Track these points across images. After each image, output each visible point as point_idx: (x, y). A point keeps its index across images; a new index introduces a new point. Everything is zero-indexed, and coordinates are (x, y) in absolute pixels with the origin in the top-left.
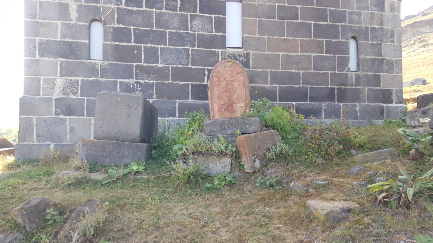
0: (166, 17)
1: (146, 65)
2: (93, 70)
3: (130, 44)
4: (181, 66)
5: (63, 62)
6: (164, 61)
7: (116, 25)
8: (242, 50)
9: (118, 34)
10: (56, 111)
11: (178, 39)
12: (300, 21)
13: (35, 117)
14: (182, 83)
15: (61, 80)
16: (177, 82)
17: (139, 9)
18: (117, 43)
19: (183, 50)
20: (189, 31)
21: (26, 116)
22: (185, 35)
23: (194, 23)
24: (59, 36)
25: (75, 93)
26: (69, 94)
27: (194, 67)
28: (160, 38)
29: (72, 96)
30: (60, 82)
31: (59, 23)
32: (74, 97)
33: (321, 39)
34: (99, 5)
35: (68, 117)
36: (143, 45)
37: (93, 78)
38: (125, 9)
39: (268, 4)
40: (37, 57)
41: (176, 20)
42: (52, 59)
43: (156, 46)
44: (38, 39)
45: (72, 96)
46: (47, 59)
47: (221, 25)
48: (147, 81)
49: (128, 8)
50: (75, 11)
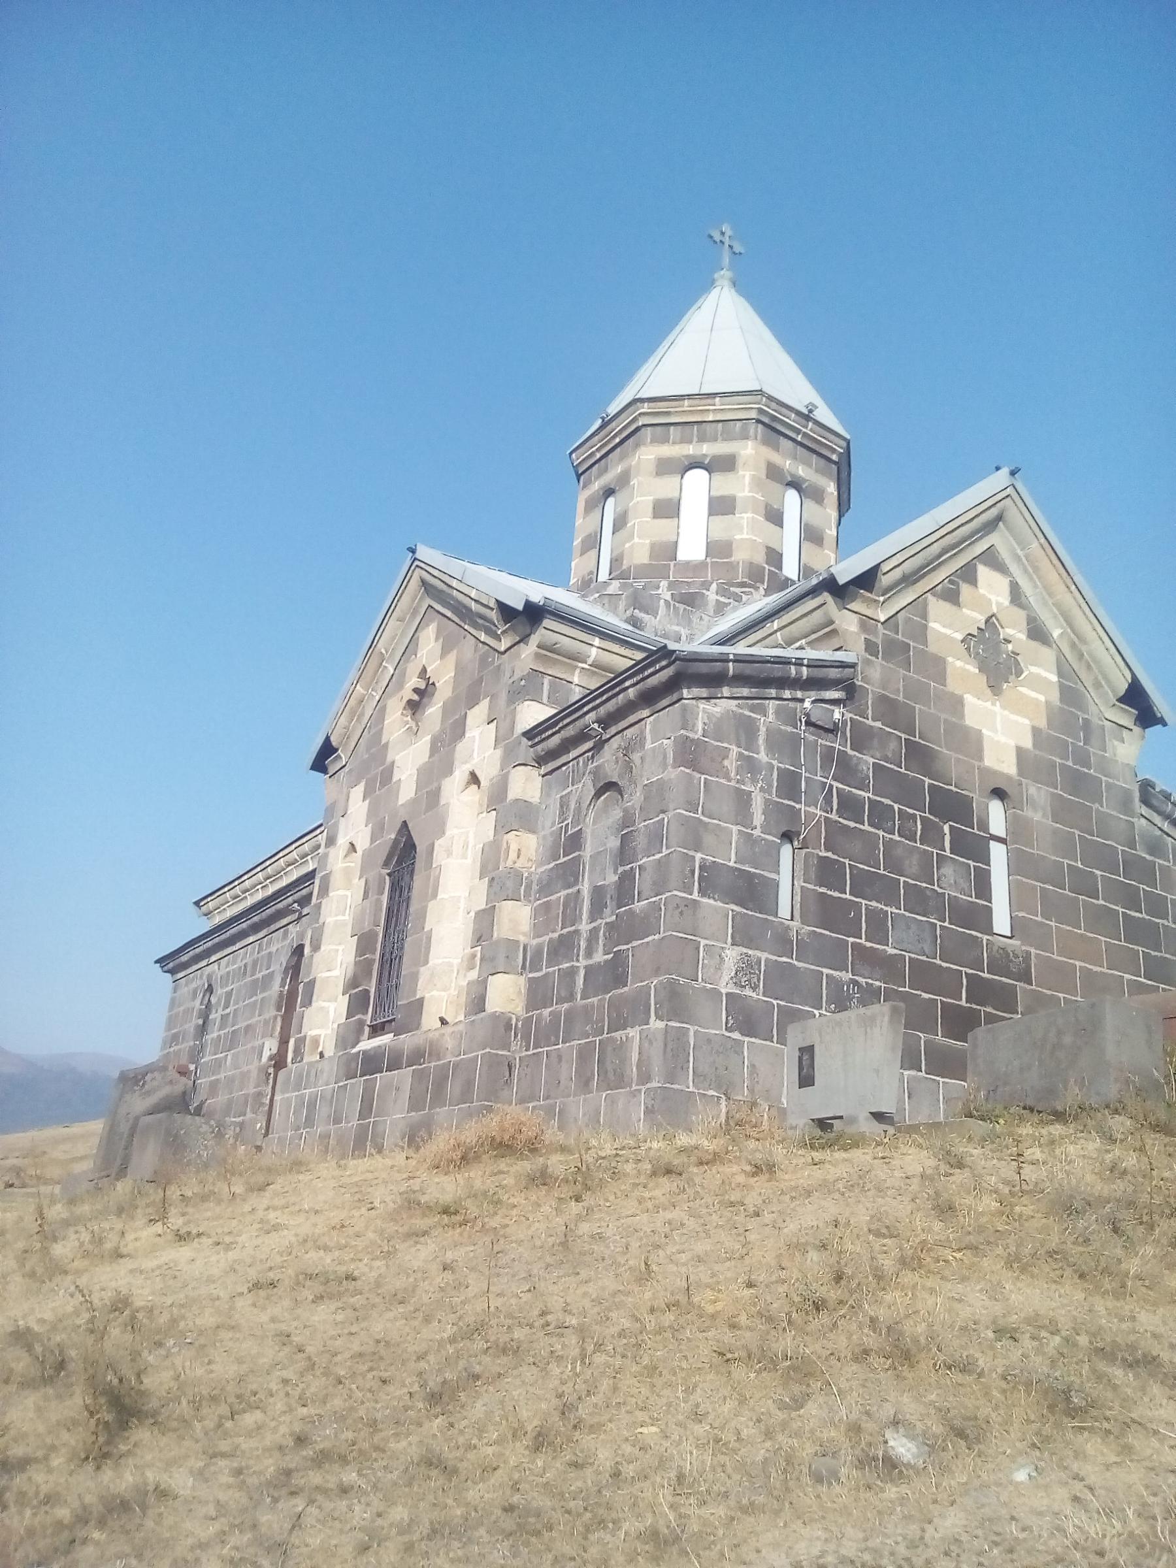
0: (899, 851)
1: (869, 944)
2: (783, 942)
3: (843, 896)
4: (924, 958)
5: (738, 913)
6: (897, 943)
7: (823, 854)
8: (1015, 942)
9: (827, 872)
10: (727, 1023)
11: (919, 901)
12: (1101, 902)
13: (692, 1029)
14: (926, 996)
15: (734, 953)
16: (919, 993)
17: (857, 825)
18: (823, 890)
19: (927, 925)
20: (936, 888)
21: (678, 1025)
22: (928, 893)
23: (942, 871)
24: (733, 858)
25: (754, 988)
26: (744, 987)
27: (945, 965)
28: (888, 892)
29: (748, 992)
30: (732, 955)
31: (735, 829)
32: (754, 995)
33: (1136, 947)
34: (798, 806)
35: (747, 1039)
36: (864, 902)
37: (784, 959)
38: (836, 821)
39: (1054, 858)
40: (695, 896)
41: (915, 860)
42: (720, 904)
43: (885, 908)
44: (699, 856)
45: (748, 992)
46: (711, 901)
47: (983, 886)
48: (870, 981)
49: (841, 820)
50: (760, 812)
